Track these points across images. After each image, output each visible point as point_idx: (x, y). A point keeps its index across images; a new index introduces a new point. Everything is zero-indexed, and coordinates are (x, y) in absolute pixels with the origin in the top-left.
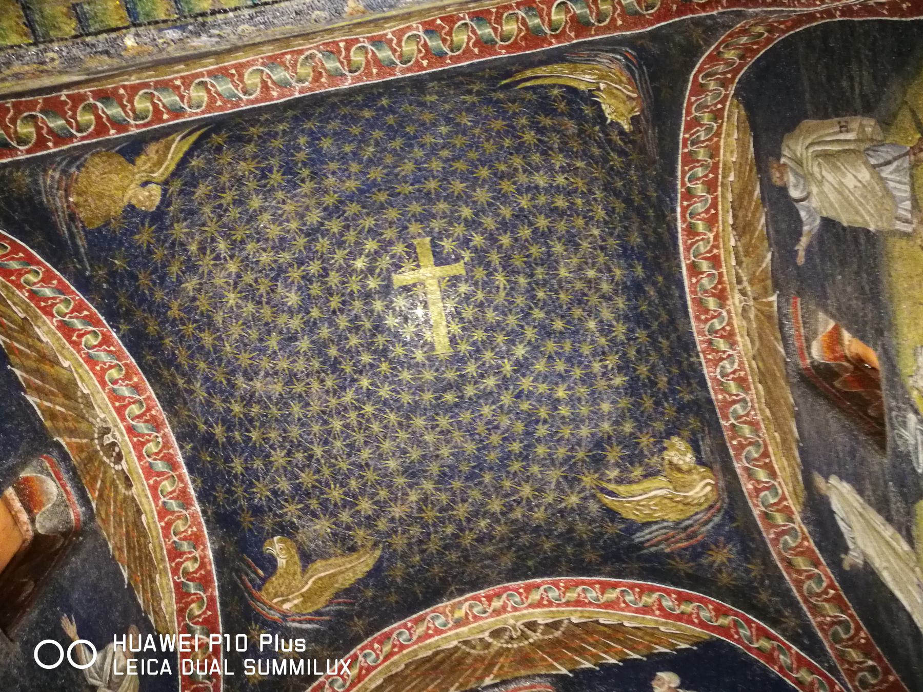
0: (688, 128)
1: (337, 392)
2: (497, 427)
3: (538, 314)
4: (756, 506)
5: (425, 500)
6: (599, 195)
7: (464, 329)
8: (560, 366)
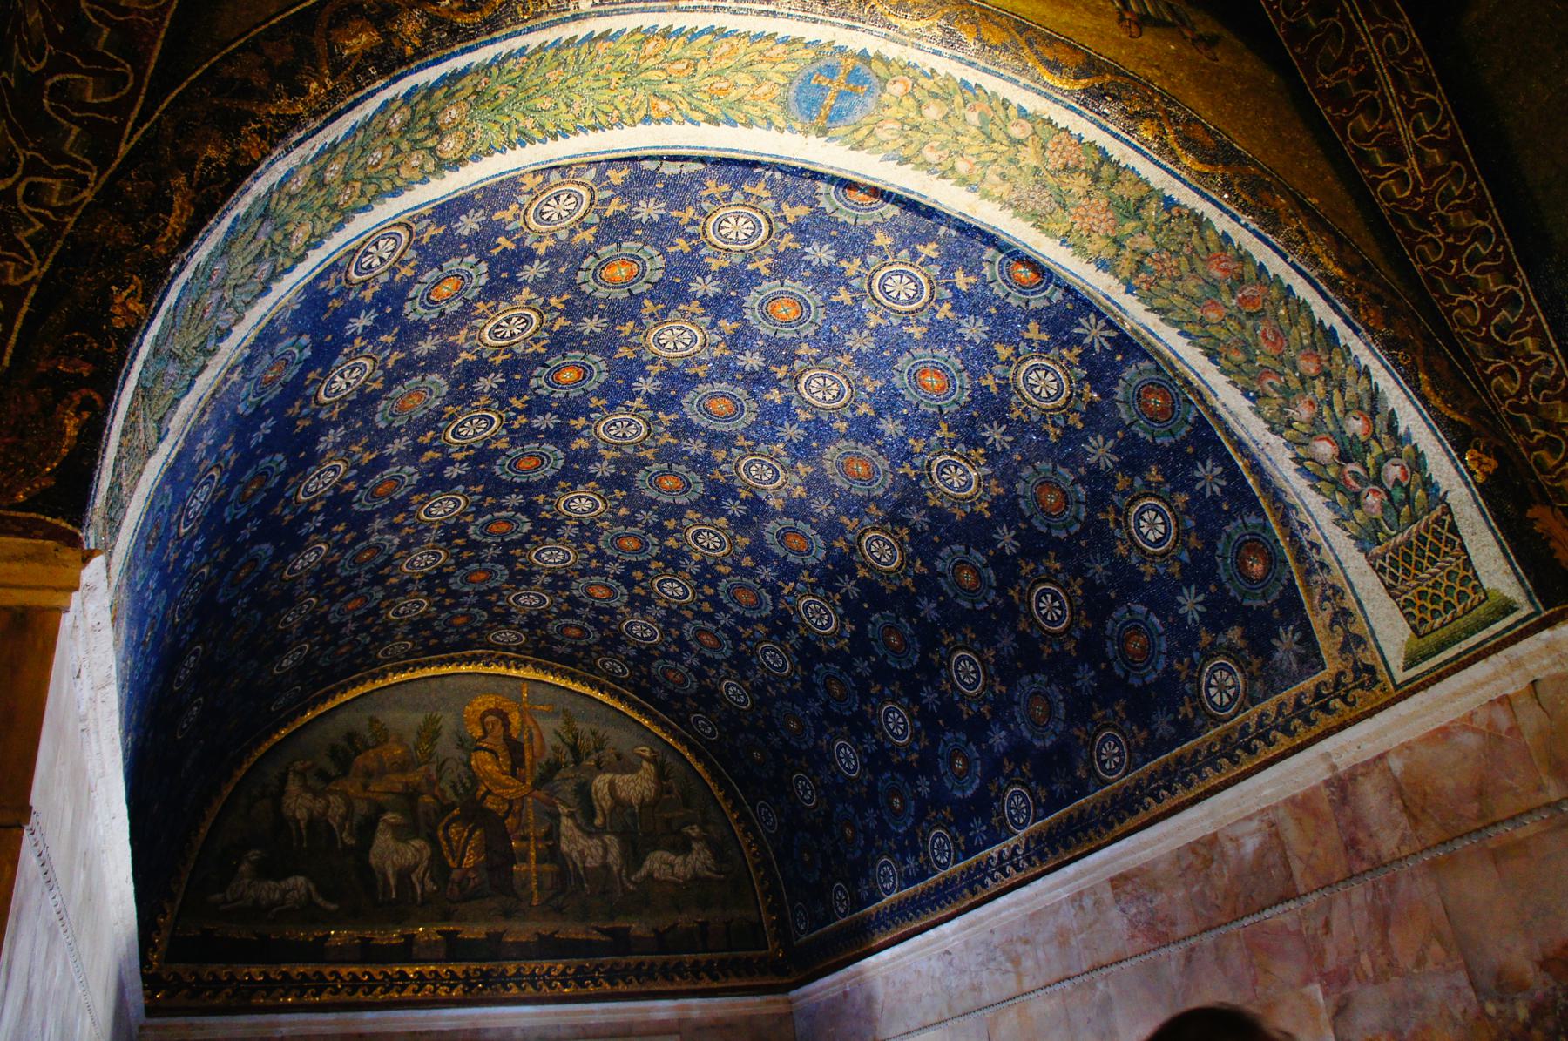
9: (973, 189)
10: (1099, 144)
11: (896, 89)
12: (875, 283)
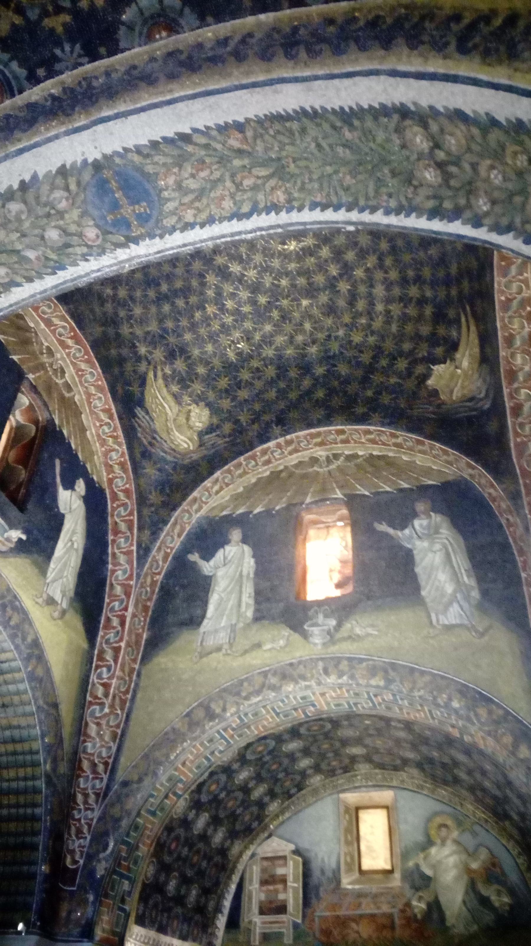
0: (441, 448)
3: (268, 281)
4: (199, 492)
6: (372, 340)
8: (230, 304)
11: (91, 233)
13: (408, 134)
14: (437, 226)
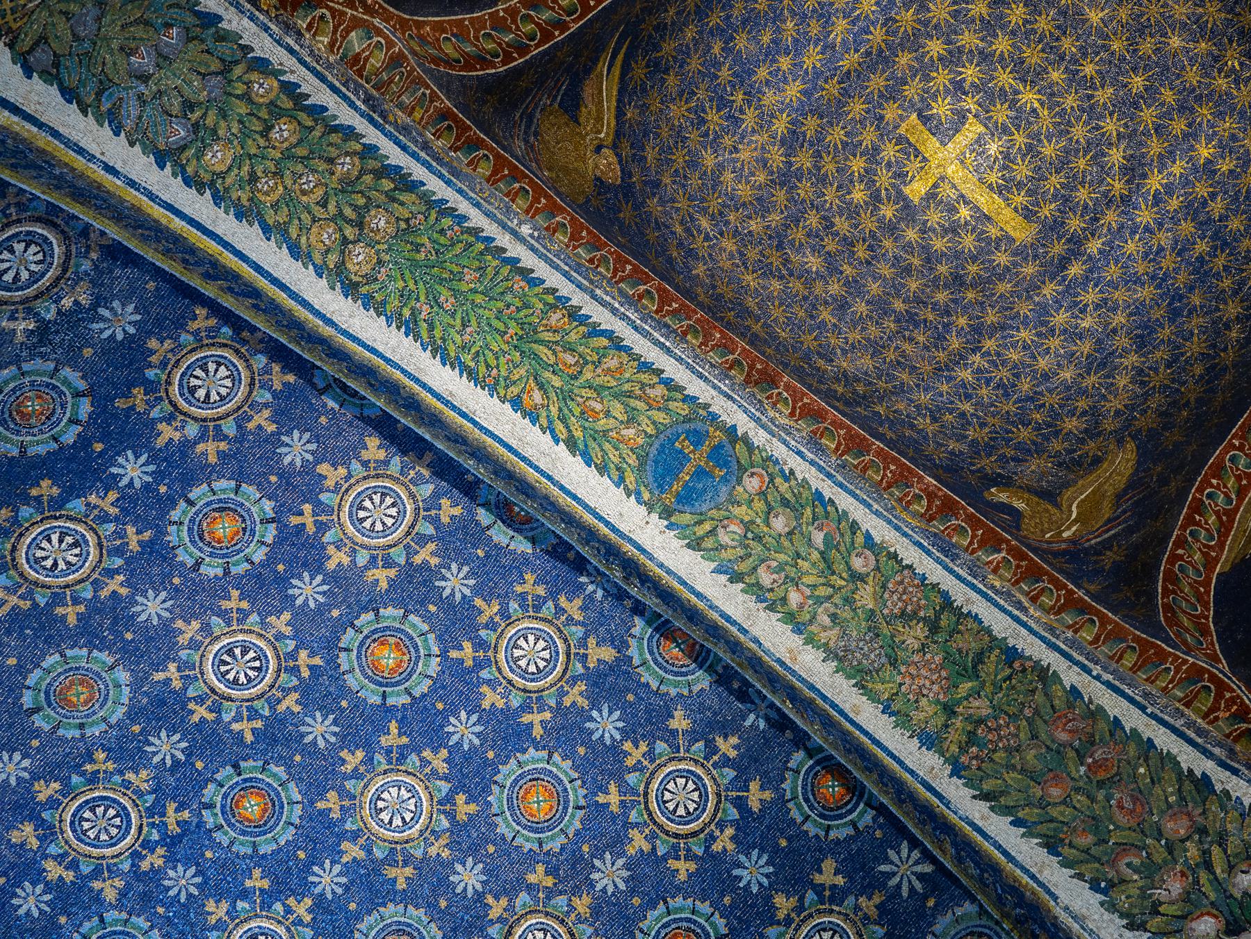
1: (939, 339)
2: (1161, 249)
3: (1104, 95)
5: (1140, 372)
7: (1030, 193)
8: (1179, 126)
9: (798, 630)
10: (943, 587)
11: (752, 484)
12: (655, 785)
13: (366, 269)
14: (419, 172)
